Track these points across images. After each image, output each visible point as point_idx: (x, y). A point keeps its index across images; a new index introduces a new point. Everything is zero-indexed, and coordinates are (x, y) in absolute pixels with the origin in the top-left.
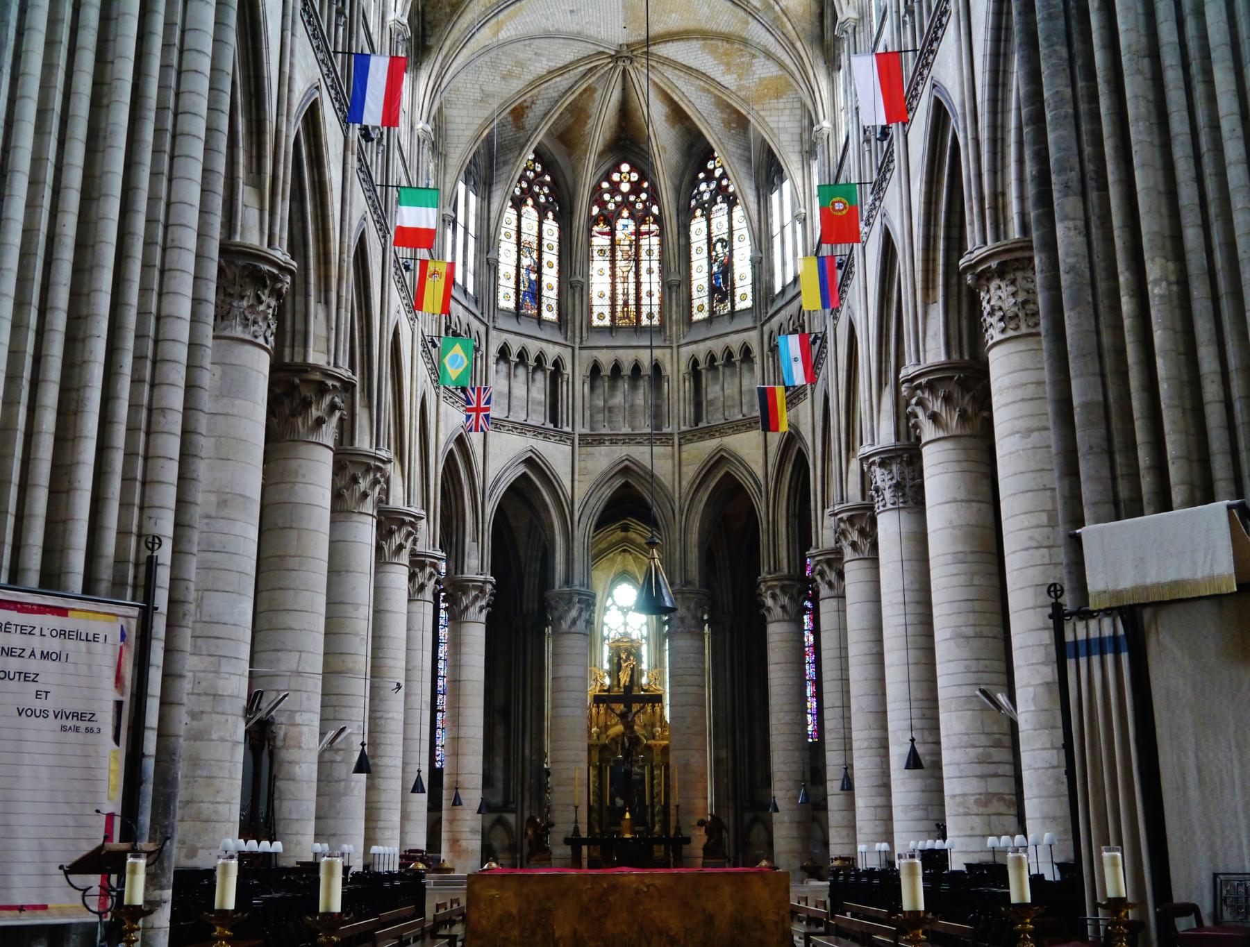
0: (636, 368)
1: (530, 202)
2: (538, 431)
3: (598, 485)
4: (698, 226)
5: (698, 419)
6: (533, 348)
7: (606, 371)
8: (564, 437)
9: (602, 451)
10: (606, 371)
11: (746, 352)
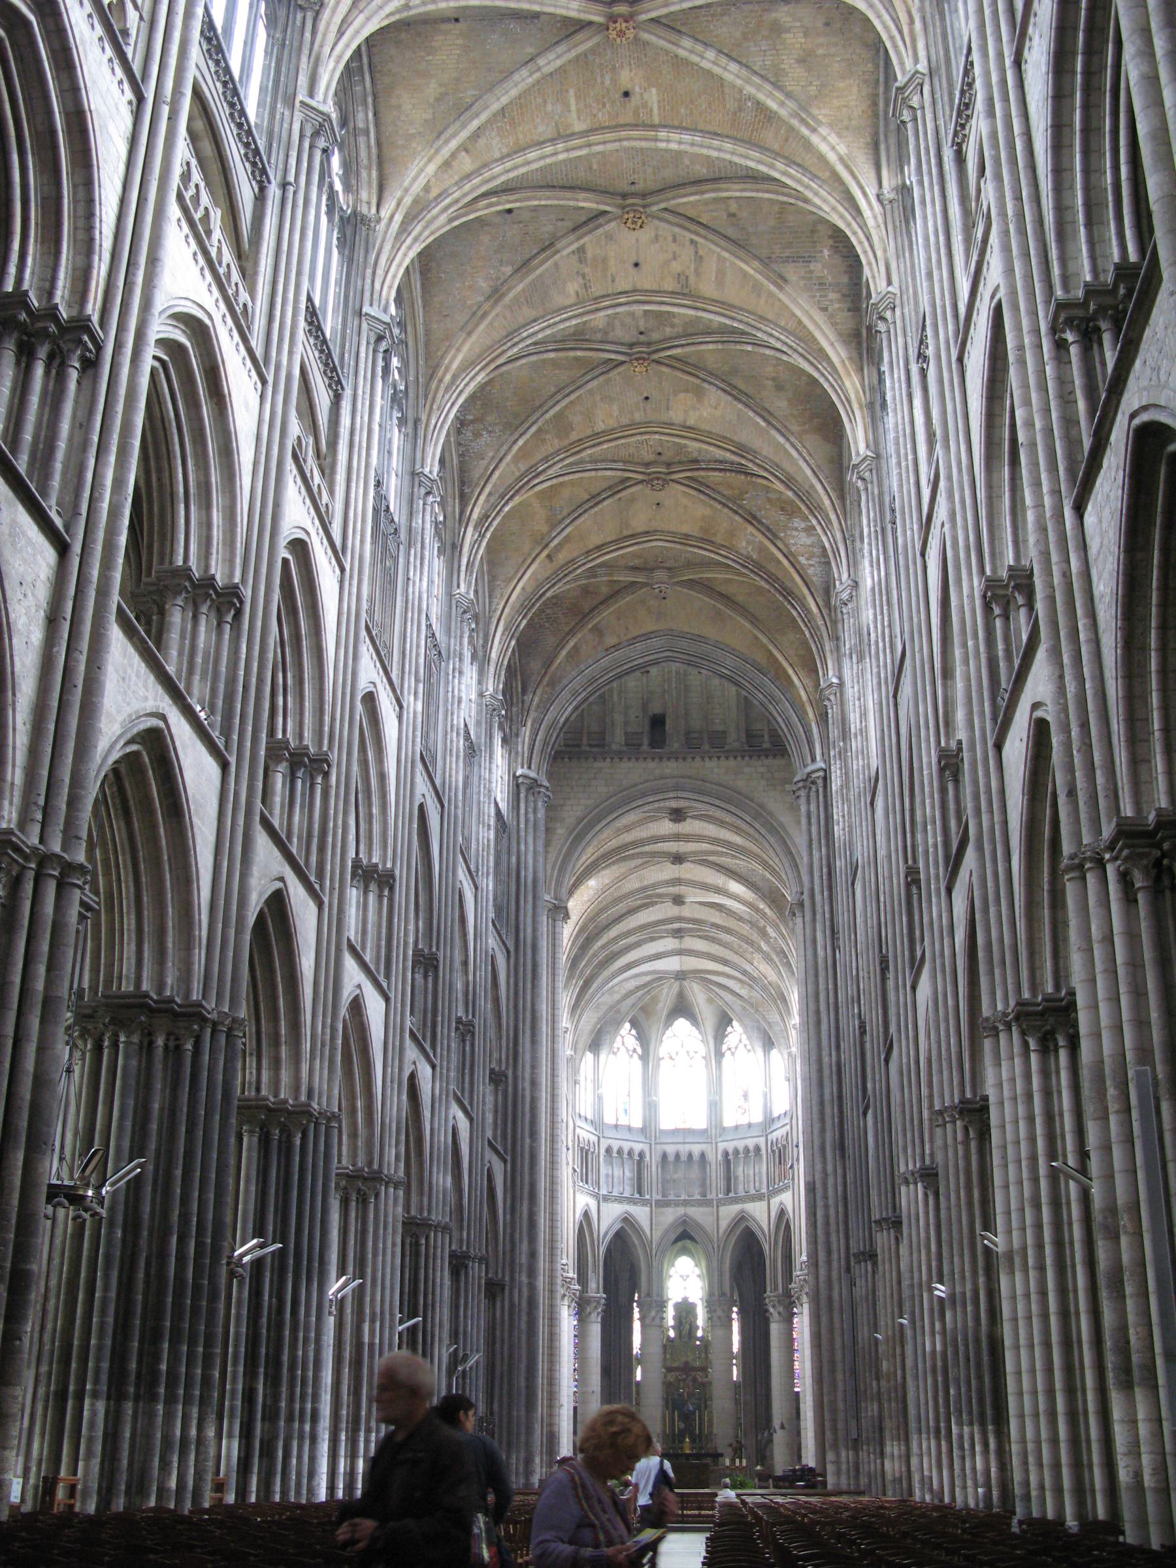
0: (690, 1155)
1: (623, 1049)
2: (631, 1201)
3: (666, 1232)
4: (727, 1060)
5: (728, 1191)
6: (626, 1146)
7: (671, 1158)
8: (645, 1203)
9: (670, 1210)
10: (671, 1158)
11: (757, 1149)
